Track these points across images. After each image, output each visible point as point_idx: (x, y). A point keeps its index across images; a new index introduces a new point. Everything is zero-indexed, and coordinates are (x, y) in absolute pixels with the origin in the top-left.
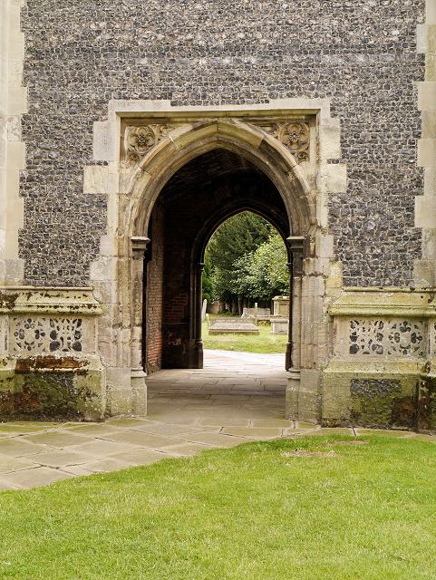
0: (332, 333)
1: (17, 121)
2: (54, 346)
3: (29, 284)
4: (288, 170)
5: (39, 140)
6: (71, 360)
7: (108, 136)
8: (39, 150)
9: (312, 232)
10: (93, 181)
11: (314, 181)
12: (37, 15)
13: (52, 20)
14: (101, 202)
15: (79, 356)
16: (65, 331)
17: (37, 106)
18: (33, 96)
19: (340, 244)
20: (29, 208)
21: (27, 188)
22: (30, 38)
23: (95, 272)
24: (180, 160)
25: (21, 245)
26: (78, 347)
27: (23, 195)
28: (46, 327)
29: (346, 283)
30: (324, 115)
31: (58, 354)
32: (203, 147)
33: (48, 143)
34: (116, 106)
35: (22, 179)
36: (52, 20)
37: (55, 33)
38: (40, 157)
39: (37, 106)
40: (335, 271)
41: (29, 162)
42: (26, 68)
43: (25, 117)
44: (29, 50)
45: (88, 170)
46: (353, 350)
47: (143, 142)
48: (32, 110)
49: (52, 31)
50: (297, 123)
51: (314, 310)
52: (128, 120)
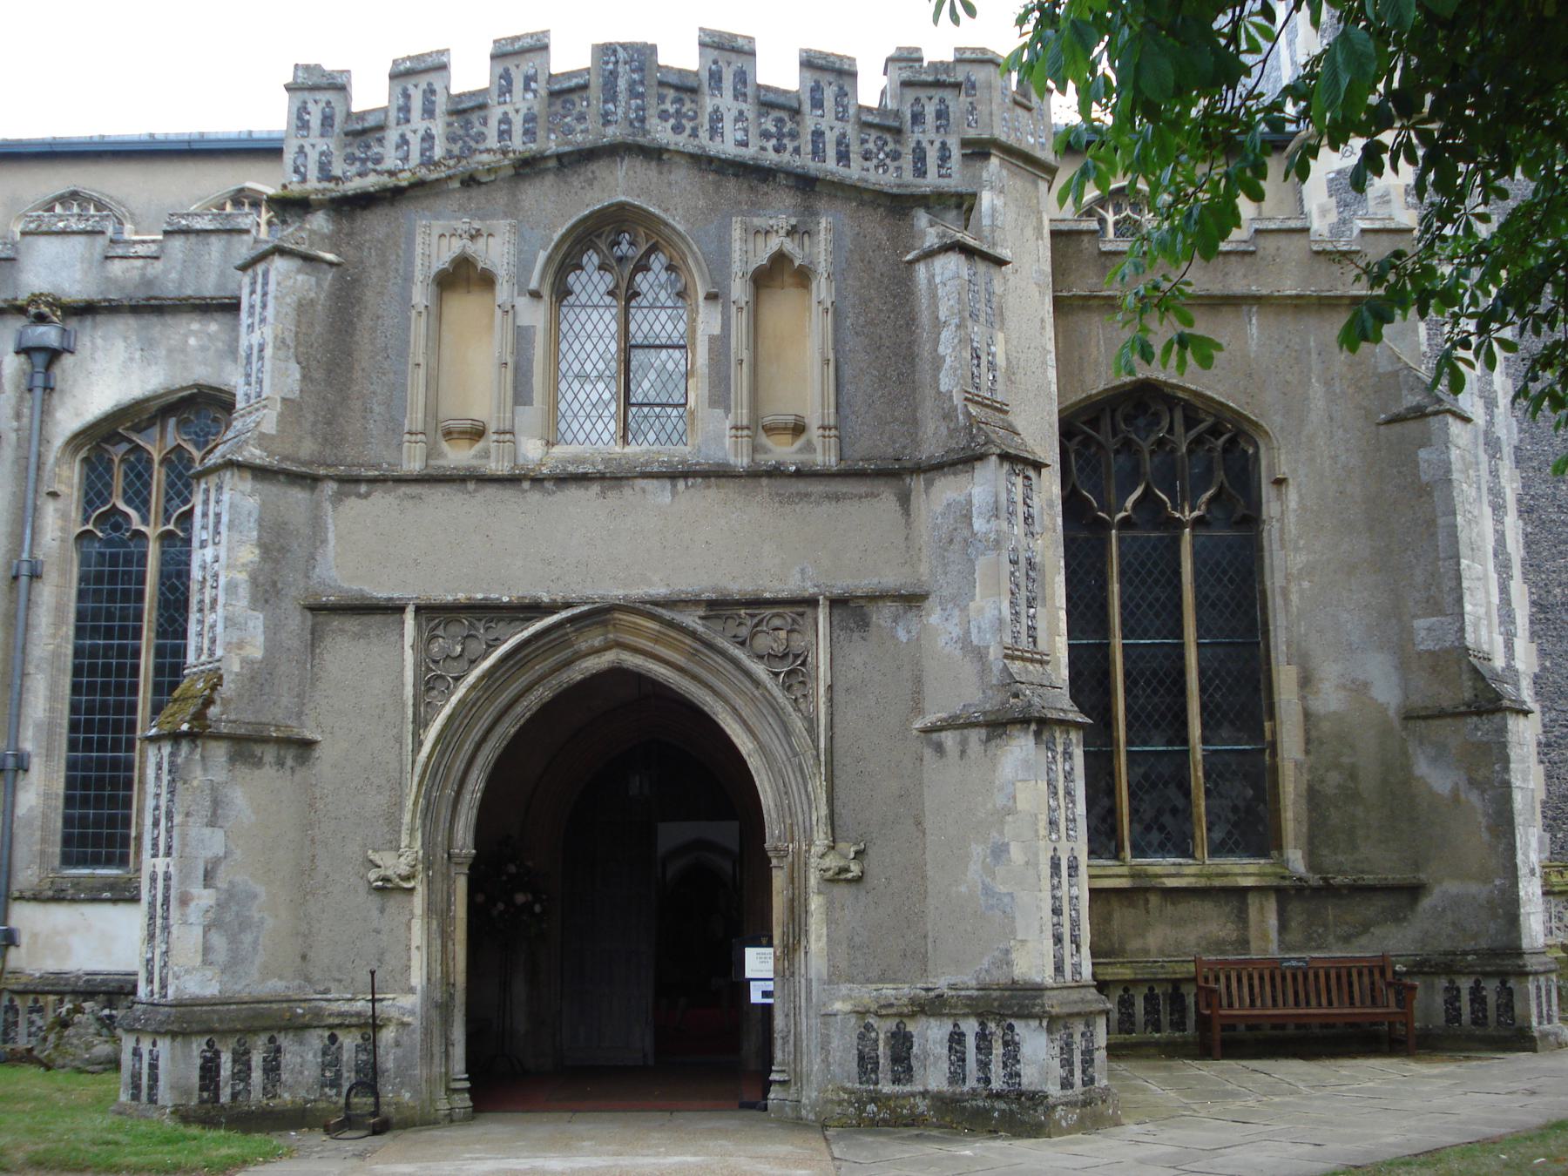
3: (1556, 860)
5: (1552, 700)
8: (1554, 713)
12: (1538, 566)
13: (1554, 572)
17: (1548, 664)
18: (1543, 653)
20: (1549, 777)
21: (1545, 754)
22: (1533, 590)
25: (1545, 817)
27: (1542, 762)
35: (1539, 744)
36: (1554, 572)
37: (1559, 585)
38: (1556, 721)
39: (1548, 664)
41: (1544, 726)
42: (1531, 622)
43: (1536, 676)
44: (1533, 603)
48: (1544, 669)
49: (1556, 583)
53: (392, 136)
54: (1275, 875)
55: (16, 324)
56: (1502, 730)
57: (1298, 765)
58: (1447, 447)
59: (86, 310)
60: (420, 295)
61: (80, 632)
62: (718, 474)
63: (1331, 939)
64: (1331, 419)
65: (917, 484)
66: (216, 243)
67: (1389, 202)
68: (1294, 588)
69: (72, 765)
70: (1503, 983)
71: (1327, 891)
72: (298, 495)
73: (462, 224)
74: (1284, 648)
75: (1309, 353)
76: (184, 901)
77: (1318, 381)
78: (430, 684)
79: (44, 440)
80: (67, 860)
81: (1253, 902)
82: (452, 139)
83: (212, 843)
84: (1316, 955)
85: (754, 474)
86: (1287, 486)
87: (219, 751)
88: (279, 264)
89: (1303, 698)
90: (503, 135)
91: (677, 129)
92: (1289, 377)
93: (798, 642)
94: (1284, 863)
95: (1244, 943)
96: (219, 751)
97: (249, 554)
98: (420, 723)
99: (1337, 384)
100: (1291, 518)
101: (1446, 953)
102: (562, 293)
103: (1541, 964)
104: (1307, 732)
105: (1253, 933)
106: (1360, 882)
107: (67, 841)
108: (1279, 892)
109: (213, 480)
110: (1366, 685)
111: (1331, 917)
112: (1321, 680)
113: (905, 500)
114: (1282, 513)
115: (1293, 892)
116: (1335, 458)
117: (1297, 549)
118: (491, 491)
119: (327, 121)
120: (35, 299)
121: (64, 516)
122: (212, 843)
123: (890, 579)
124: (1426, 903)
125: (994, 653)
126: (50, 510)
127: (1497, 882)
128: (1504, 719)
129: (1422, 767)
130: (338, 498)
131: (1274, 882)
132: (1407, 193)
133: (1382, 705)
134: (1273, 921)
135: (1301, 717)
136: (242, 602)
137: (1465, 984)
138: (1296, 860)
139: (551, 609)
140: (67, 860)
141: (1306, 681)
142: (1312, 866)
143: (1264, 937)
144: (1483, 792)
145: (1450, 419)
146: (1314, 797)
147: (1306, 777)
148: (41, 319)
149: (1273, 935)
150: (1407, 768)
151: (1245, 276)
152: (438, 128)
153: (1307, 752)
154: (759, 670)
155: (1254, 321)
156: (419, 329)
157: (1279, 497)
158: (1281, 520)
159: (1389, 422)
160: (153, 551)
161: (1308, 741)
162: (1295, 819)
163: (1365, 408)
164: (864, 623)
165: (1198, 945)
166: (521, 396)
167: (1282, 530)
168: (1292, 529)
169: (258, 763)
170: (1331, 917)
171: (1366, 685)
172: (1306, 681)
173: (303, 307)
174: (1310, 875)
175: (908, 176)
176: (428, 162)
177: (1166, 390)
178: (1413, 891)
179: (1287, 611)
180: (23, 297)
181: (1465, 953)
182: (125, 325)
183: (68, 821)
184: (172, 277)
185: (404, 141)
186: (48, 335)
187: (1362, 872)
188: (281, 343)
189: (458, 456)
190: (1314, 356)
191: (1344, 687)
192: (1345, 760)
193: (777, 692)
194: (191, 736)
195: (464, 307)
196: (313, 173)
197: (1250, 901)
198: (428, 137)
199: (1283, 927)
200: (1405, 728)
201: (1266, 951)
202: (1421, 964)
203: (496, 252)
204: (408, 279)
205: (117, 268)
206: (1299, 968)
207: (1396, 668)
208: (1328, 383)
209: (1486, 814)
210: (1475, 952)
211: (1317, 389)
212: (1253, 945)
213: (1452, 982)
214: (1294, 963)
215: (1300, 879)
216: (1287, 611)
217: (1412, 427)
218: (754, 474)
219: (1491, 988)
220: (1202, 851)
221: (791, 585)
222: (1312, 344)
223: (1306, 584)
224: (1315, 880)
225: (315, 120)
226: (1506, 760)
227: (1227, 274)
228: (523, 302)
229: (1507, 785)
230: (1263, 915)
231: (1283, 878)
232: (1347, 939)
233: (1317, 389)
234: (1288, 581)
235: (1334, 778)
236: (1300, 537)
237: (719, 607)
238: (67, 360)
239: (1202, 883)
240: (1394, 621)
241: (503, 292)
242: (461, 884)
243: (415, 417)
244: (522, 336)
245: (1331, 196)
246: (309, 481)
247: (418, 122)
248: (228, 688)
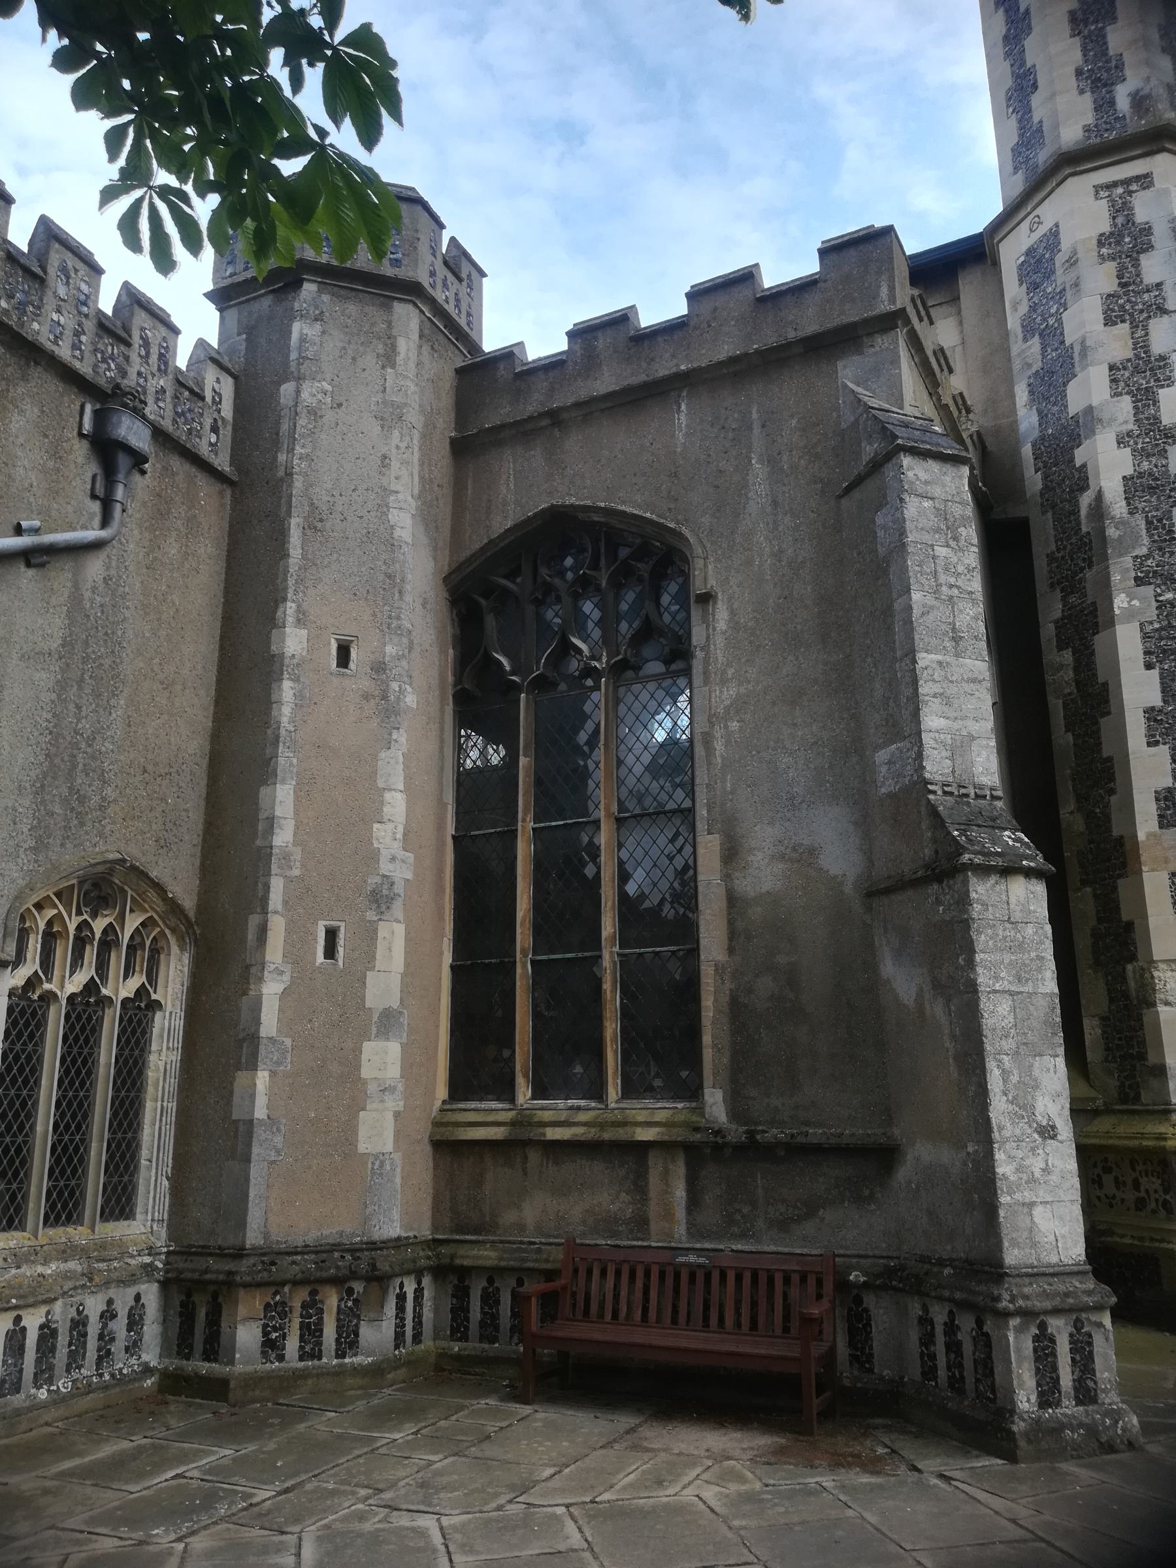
54: (686, 1124)
56: (964, 901)
57: (719, 969)
58: (902, 500)
63: (760, 1224)
64: (775, 503)
67: (1076, 261)
68: (718, 732)
70: (980, 1323)
74: (705, 812)
75: (750, 428)
77: (760, 461)
81: (655, 1165)
84: (739, 1247)
86: (715, 603)
89: (727, 877)
92: (722, 465)
94: (700, 1110)
95: (641, 1223)
99: (785, 458)
100: (720, 641)
101: (924, 1259)
103: (1045, 1295)
104: (731, 923)
105: (653, 1209)
106: (801, 1139)
110: (812, 851)
111: (760, 1191)
112: (751, 851)
114: (708, 638)
115: (708, 1151)
116: (778, 555)
117: (724, 682)
124: (903, 1173)
127: (970, 1149)
128: (966, 882)
129: (888, 968)
131: (679, 1135)
132: (1100, 244)
133: (836, 877)
134: (680, 1192)
135: (724, 904)
137: (939, 1316)
138: (715, 1102)
141: (731, 854)
142: (735, 1114)
143: (668, 1216)
144: (948, 1000)
145: (907, 461)
147: (728, 985)
149: (680, 1213)
150: (872, 967)
151: (673, 356)
153: (731, 950)
155: (683, 407)
157: (705, 620)
158: (705, 648)
159: (848, 490)
161: (732, 935)
162: (714, 1046)
163: (821, 481)
165: (584, 1222)
167: (706, 661)
168: (719, 651)
170: (760, 1191)
171: (812, 851)
172: (731, 854)
174: (734, 1127)
177: (581, 516)
179: (709, 763)
181: (941, 1263)
187: (807, 1123)
190: (757, 430)
191: (782, 857)
192: (782, 959)
197: (650, 1163)
199: (693, 1202)
200: (869, 909)
201: (670, 1236)
202: (890, 1272)
206: (700, 1266)
207: (856, 824)
208: (772, 461)
209: (953, 1037)
210: (951, 1262)
211: (758, 467)
212: (654, 1227)
213: (925, 1309)
214: (692, 1258)
215: (718, 1132)
216: (709, 763)
217: (870, 485)
219: (966, 1323)
222: (755, 416)
223: (734, 725)
224: (736, 1133)
226: (969, 949)
227: (652, 360)
229: (972, 988)
230: (667, 1185)
231: (697, 1129)
232: (783, 1225)
233: (758, 467)
234: (712, 725)
235: (766, 985)
236: (729, 664)
239: (592, 1134)
240: (854, 759)
245: (1021, 285)
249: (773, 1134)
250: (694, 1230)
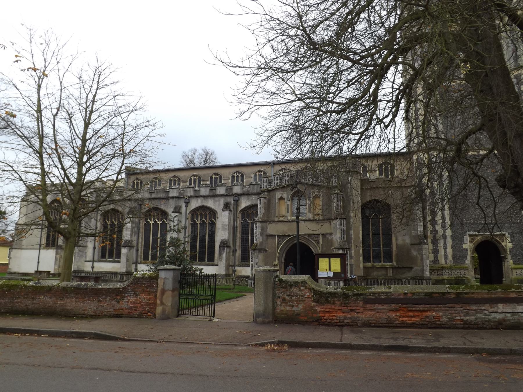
0: (512, 272)
1: (450, 236)
2: (461, 275)
4: (500, 244)
6: (464, 277)
7: (467, 239)
9: (506, 254)
10: (465, 246)
11: (506, 246)
14: (467, 250)
15: (466, 276)
16: (462, 272)
19: (512, 257)
20: (453, 251)
23: (467, 262)
24: (479, 242)
26: (465, 275)
28: (459, 271)
29: (514, 263)
30: (507, 235)
31: (461, 276)
32: (484, 240)
33: (455, 240)
34: (468, 234)
40: (511, 261)
45: (464, 244)
46: (517, 275)
47: (472, 239)
50: (501, 236)
51: (508, 268)
52: (470, 236)
53: (273, 183)
55: (233, 197)
59: (241, 195)
60: (277, 201)
61: (242, 234)
62: (309, 220)
65: (332, 221)
66: (256, 186)
69: (242, 250)
71: (399, 268)
72: (265, 224)
73: (281, 193)
76: (254, 267)
78: (279, 244)
79: (237, 211)
80: (242, 262)
81: (388, 268)
82: (280, 183)
83: (257, 261)
85: (314, 220)
87: (257, 251)
88: (262, 199)
90: (285, 182)
91: (305, 180)
93: (318, 239)
94: (393, 264)
95: (387, 274)
96: (257, 251)
97: (260, 231)
98: (278, 248)
102: (292, 200)
105: (388, 273)
107: (241, 259)
108: (392, 268)
109: (256, 223)
110: (405, 240)
113: (330, 223)
118: (285, 223)
119: (266, 181)
120: (235, 194)
121: (240, 220)
122: (257, 261)
123: (328, 232)
124: (413, 270)
125: (339, 241)
126: (238, 220)
129: (413, 251)
130: (269, 224)
134: (391, 272)
136: (259, 236)
138: (395, 263)
139: (291, 236)
140: (242, 262)
141: (397, 239)
143: (390, 274)
146: (397, 255)
148: (236, 197)
152: (278, 181)
154: (314, 242)
156: (277, 205)
160: (250, 224)
161: (397, 247)
164: (325, 237)
166: (288, 212)
169: (261, 252)
171: (405, 240)
172: (397, 239)
173: (265, 203)
175: (331, 184)
176: (277, 186)
178: (412, 268)
180: (234, 193)
182: (246, 197)
183: (241, 257)
184: (251, 191)
185: (275, 183)
186: (237, 198)
188: (262, 208)
189: (281, 219)
193: (316, 245)
194: (255, 250)
195: (282, 202)
196: (265, 187)
198: (277, 183)
203: (285, 196)
204: (276, 199)
205: (244, 189)
218: (314, 220)
220: (372, 262)
221: (317, 232)
224: (397, 266)
225: (265, 181)
228: (288, 201)
237: (310, 235)
238: (239, 201)
241: (286, 200)
242: (283, 265)
243: (277, 215)
244: (288, 205)
246: (266, 222)
247: (276, 181)
248: (258, 245)
249: (401, 266)
250: (393, 275)
